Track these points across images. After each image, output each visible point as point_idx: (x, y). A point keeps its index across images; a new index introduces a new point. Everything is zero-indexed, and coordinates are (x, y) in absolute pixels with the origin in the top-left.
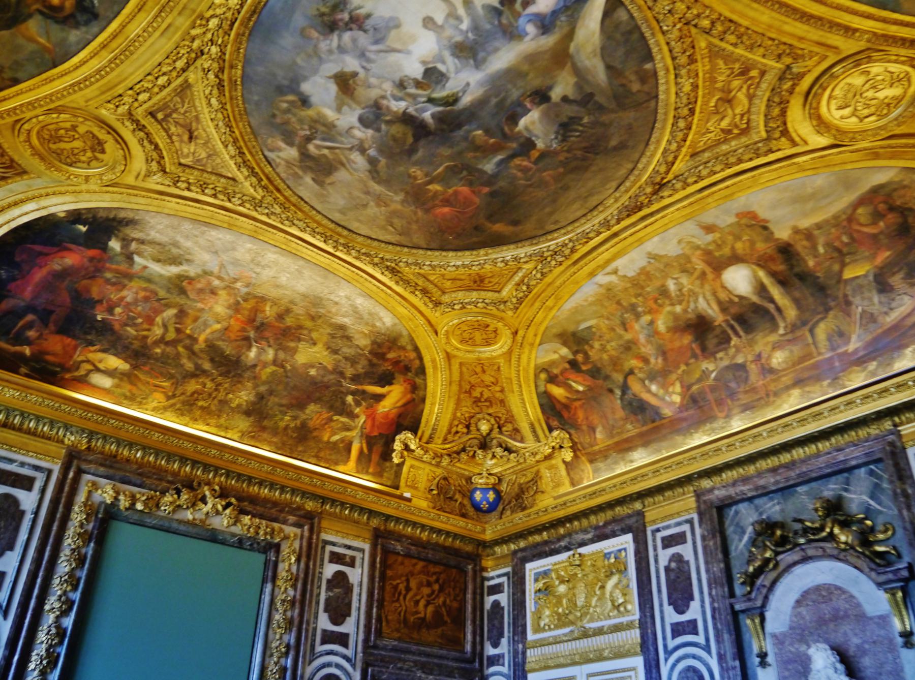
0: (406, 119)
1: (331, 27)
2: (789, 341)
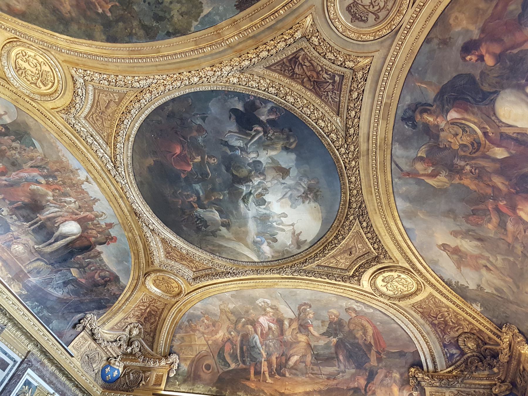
0: (247, 179)
1: (310, 189)
2: (31, 251)
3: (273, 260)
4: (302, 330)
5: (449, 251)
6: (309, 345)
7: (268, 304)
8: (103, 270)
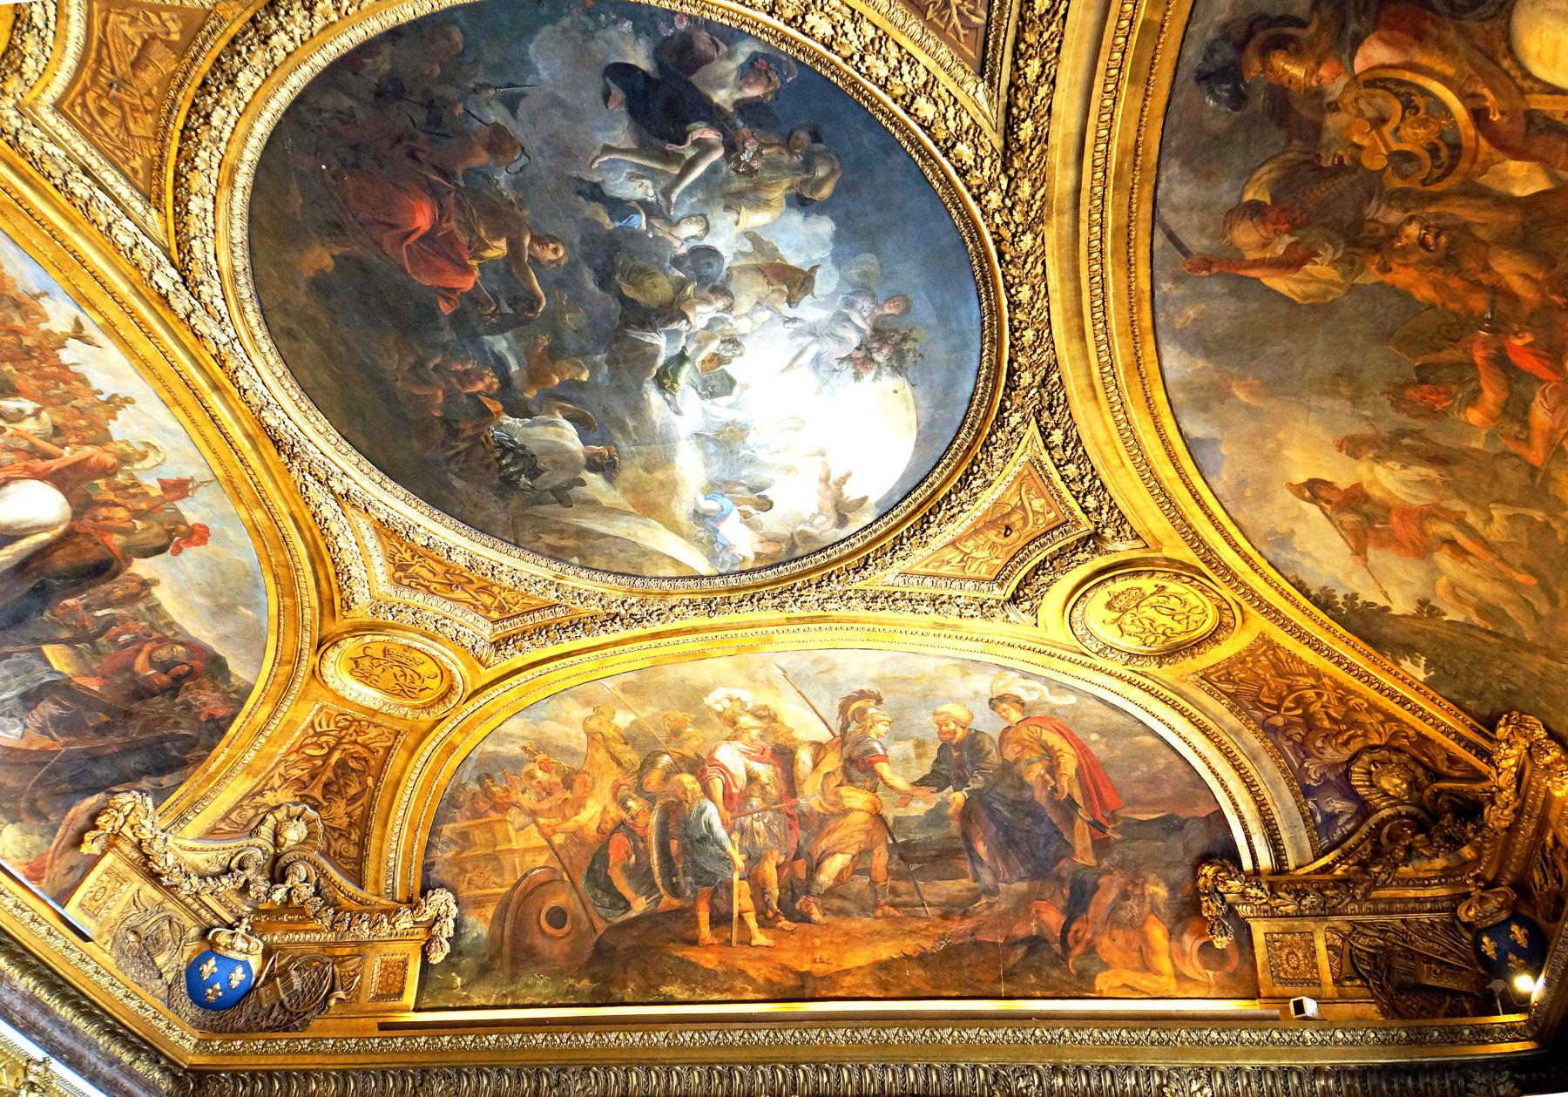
0: (671, 311)
1: (880, 333)
3: (759, 565)
4: (855, 773)
5: (1328, 502)
6: (878, 818)
7: (743, 704)
8: (163, 641)
